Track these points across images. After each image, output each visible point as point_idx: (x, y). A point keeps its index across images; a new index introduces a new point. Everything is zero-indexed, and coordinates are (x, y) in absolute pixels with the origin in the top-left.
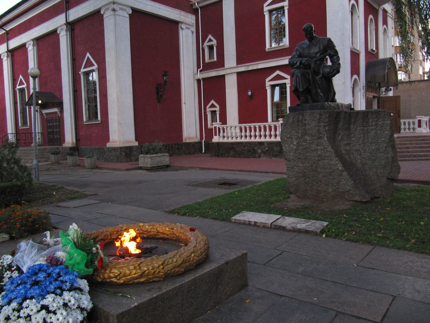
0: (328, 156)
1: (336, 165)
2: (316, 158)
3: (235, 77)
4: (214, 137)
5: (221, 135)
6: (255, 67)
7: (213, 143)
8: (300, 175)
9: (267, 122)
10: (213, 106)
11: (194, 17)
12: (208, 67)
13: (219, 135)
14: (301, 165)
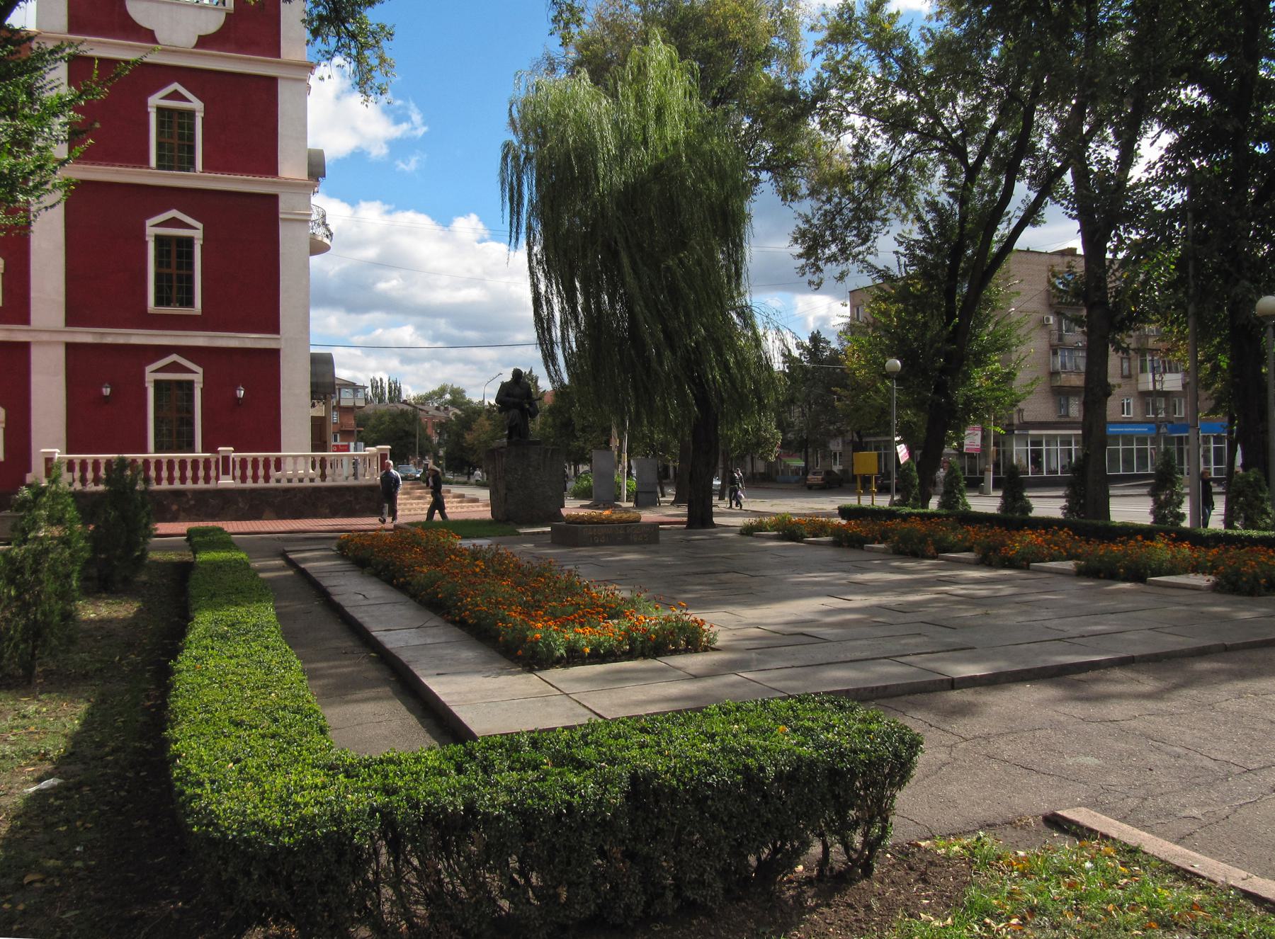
3: (61, 352)
6: (121, 340)
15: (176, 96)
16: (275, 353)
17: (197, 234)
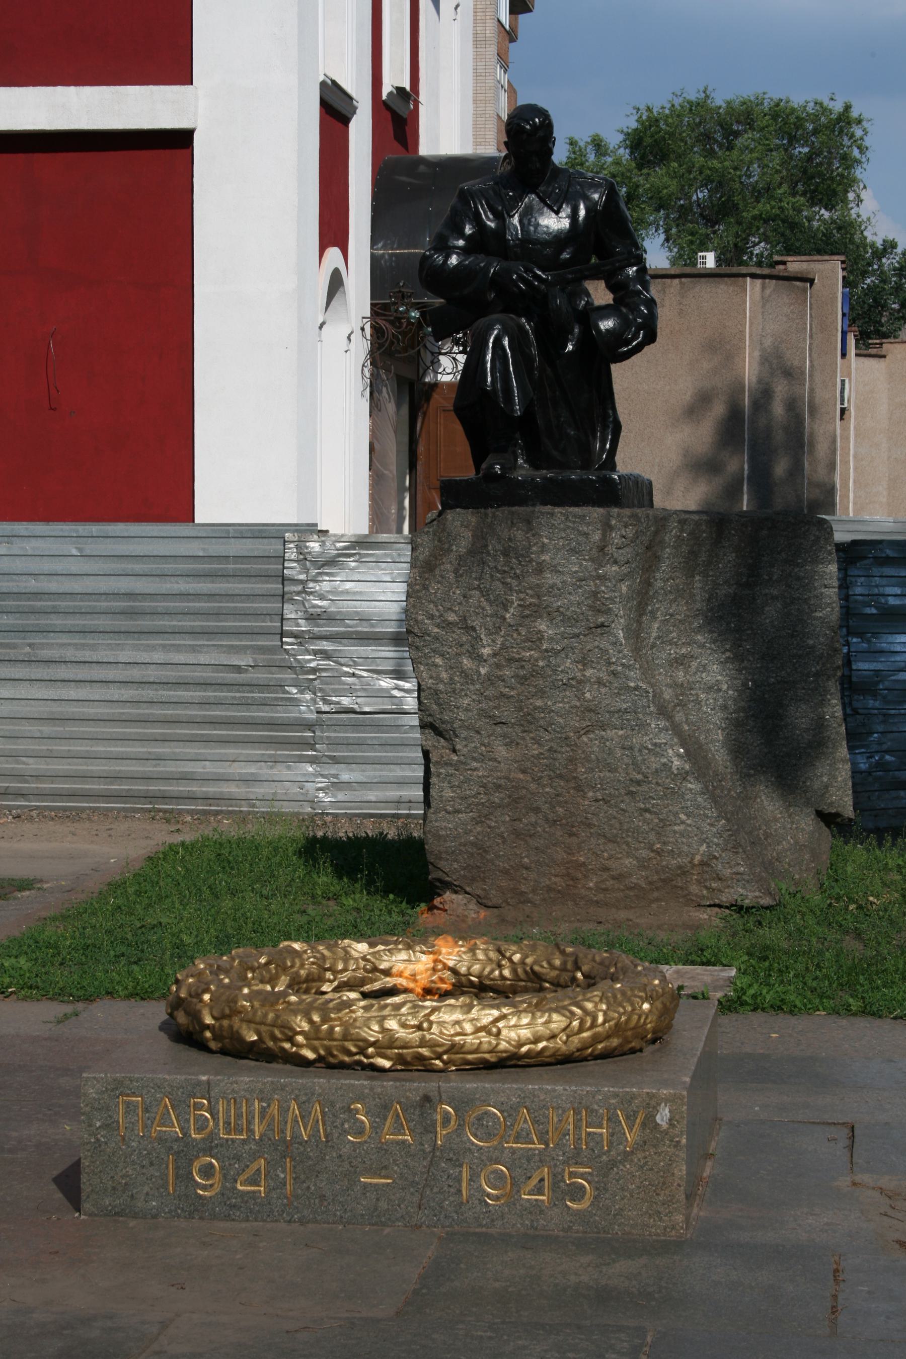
0: (626, 711)
1: (657, 749)
2: (575, 722)
8: (496, 798)
14: (501, 751)
16: (180, 140)
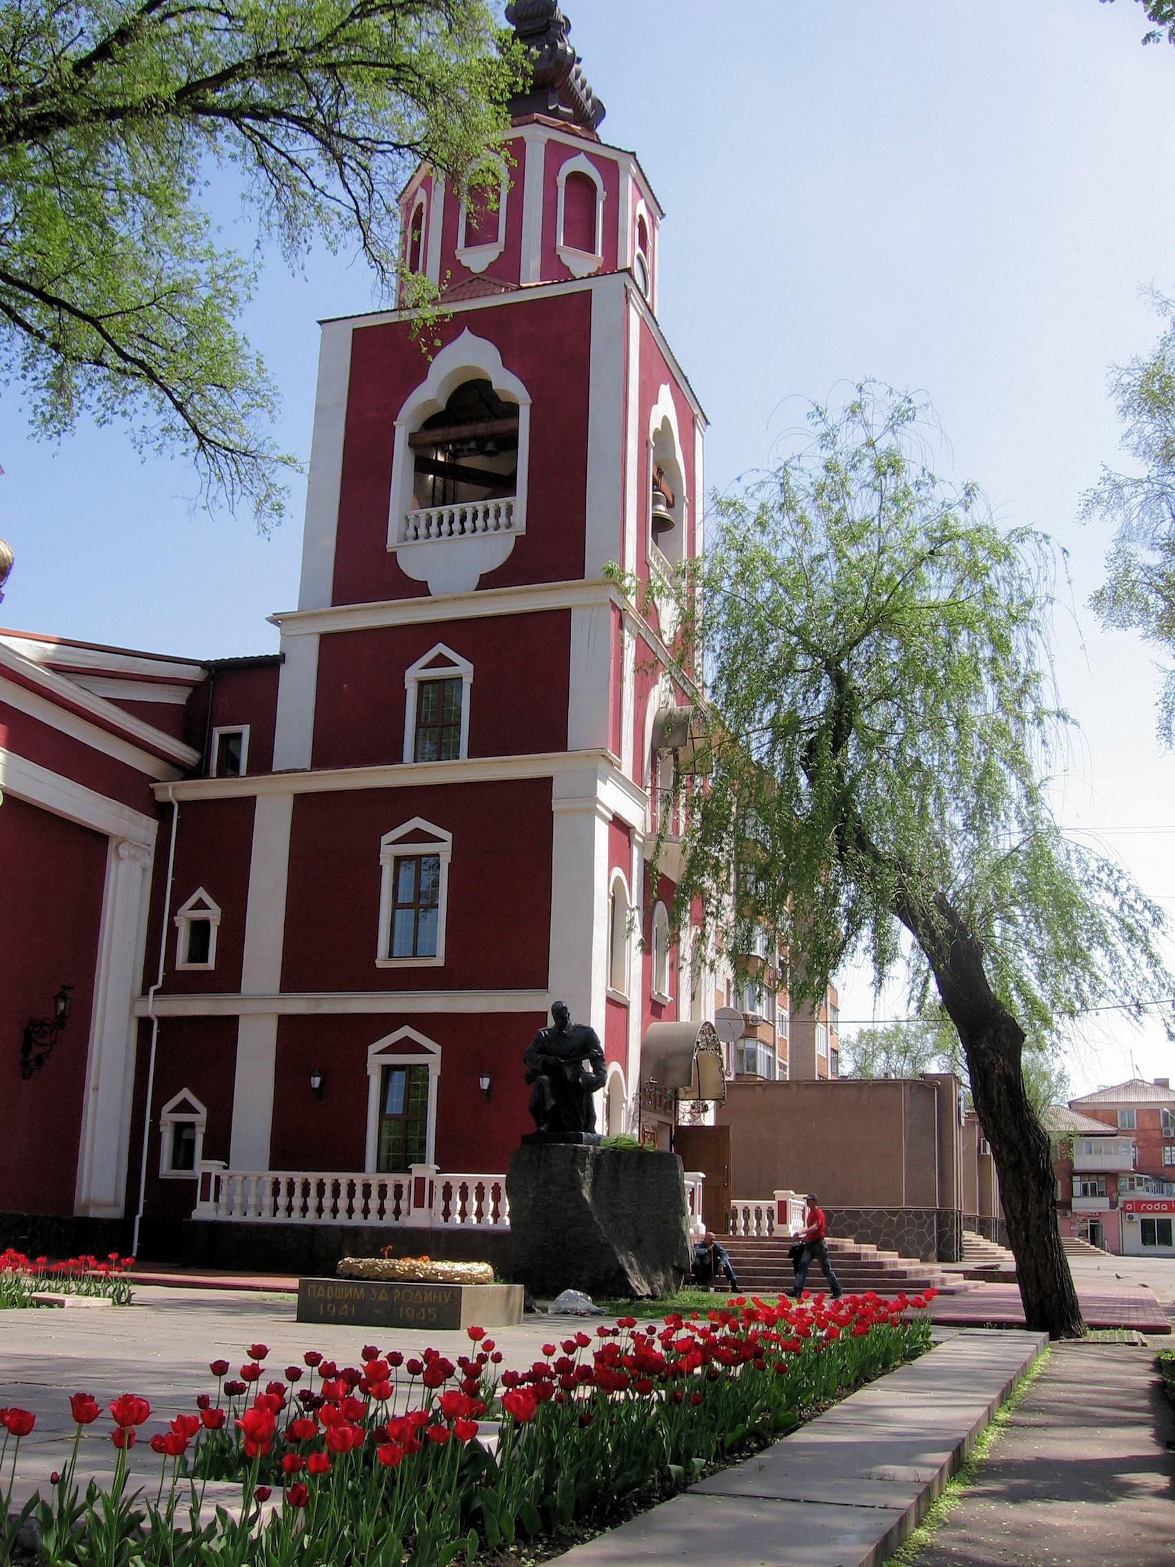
4: (199, 1204)
5: (222, 1198)
7: (196, 1223)
9: (361, 1168)
10: (185, 1107)
11: (153, 824)
12: (179, 984)
13: (216, 1200)
15: (441, 661)
17: (444, 851)
